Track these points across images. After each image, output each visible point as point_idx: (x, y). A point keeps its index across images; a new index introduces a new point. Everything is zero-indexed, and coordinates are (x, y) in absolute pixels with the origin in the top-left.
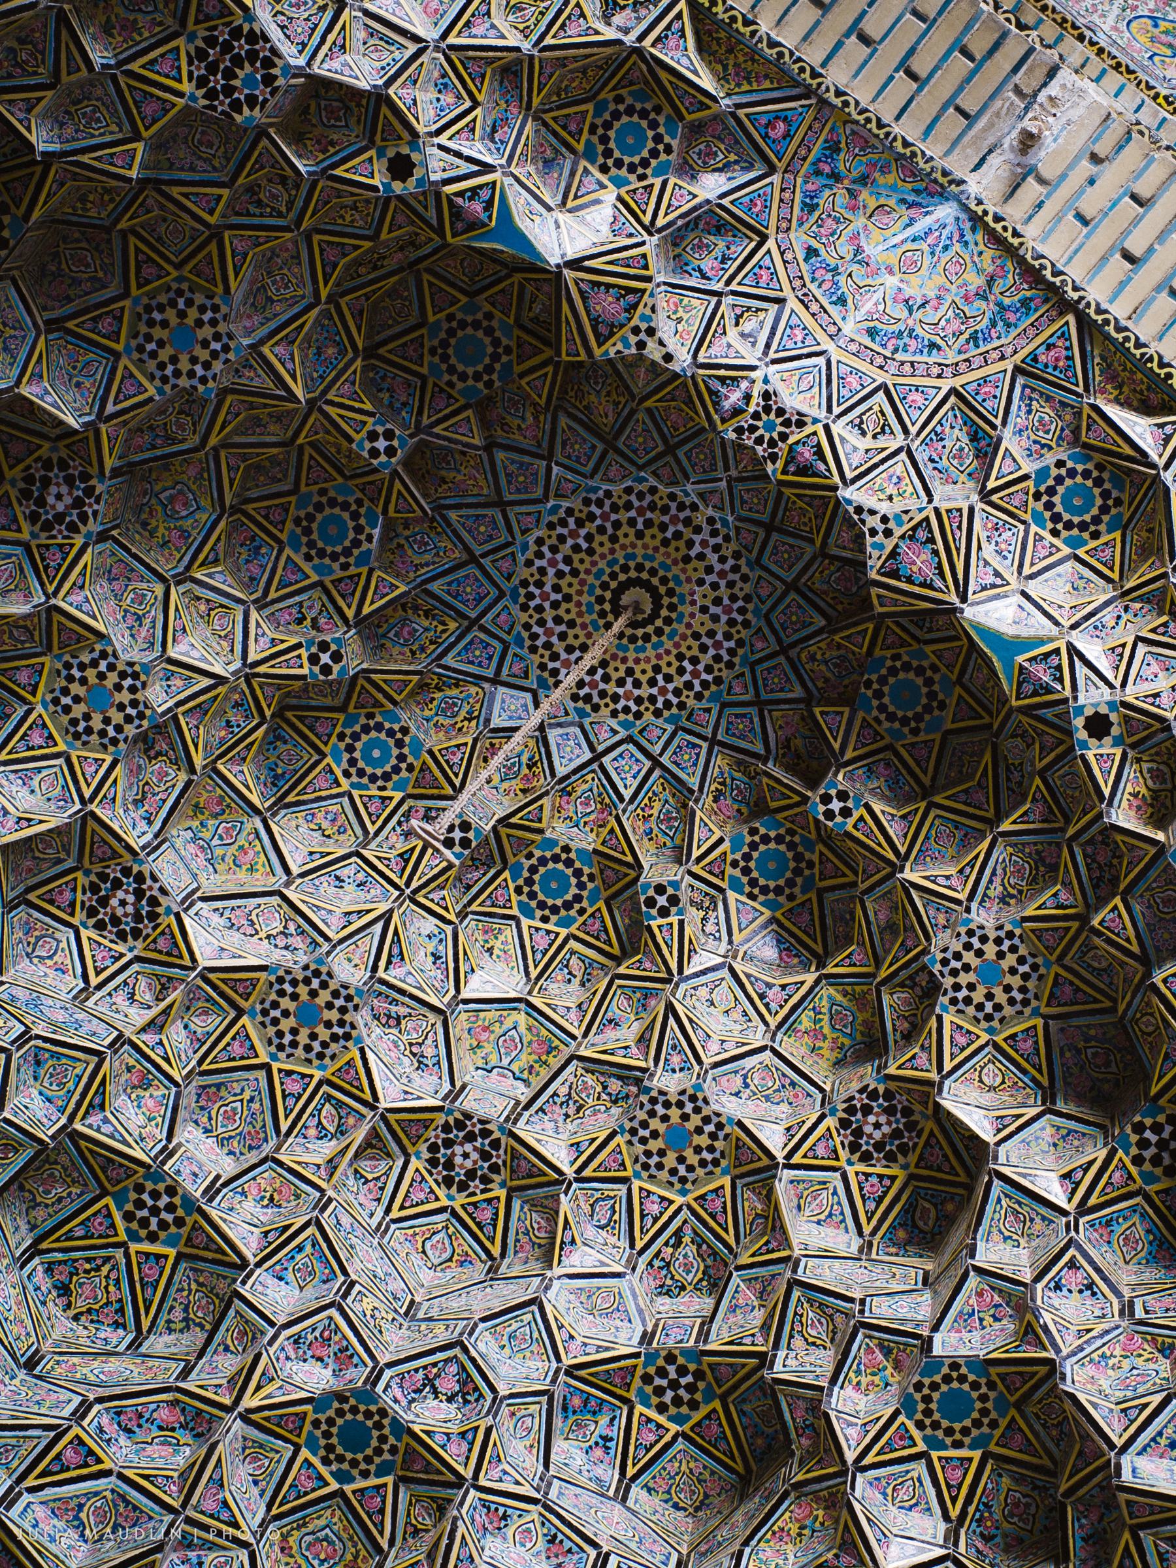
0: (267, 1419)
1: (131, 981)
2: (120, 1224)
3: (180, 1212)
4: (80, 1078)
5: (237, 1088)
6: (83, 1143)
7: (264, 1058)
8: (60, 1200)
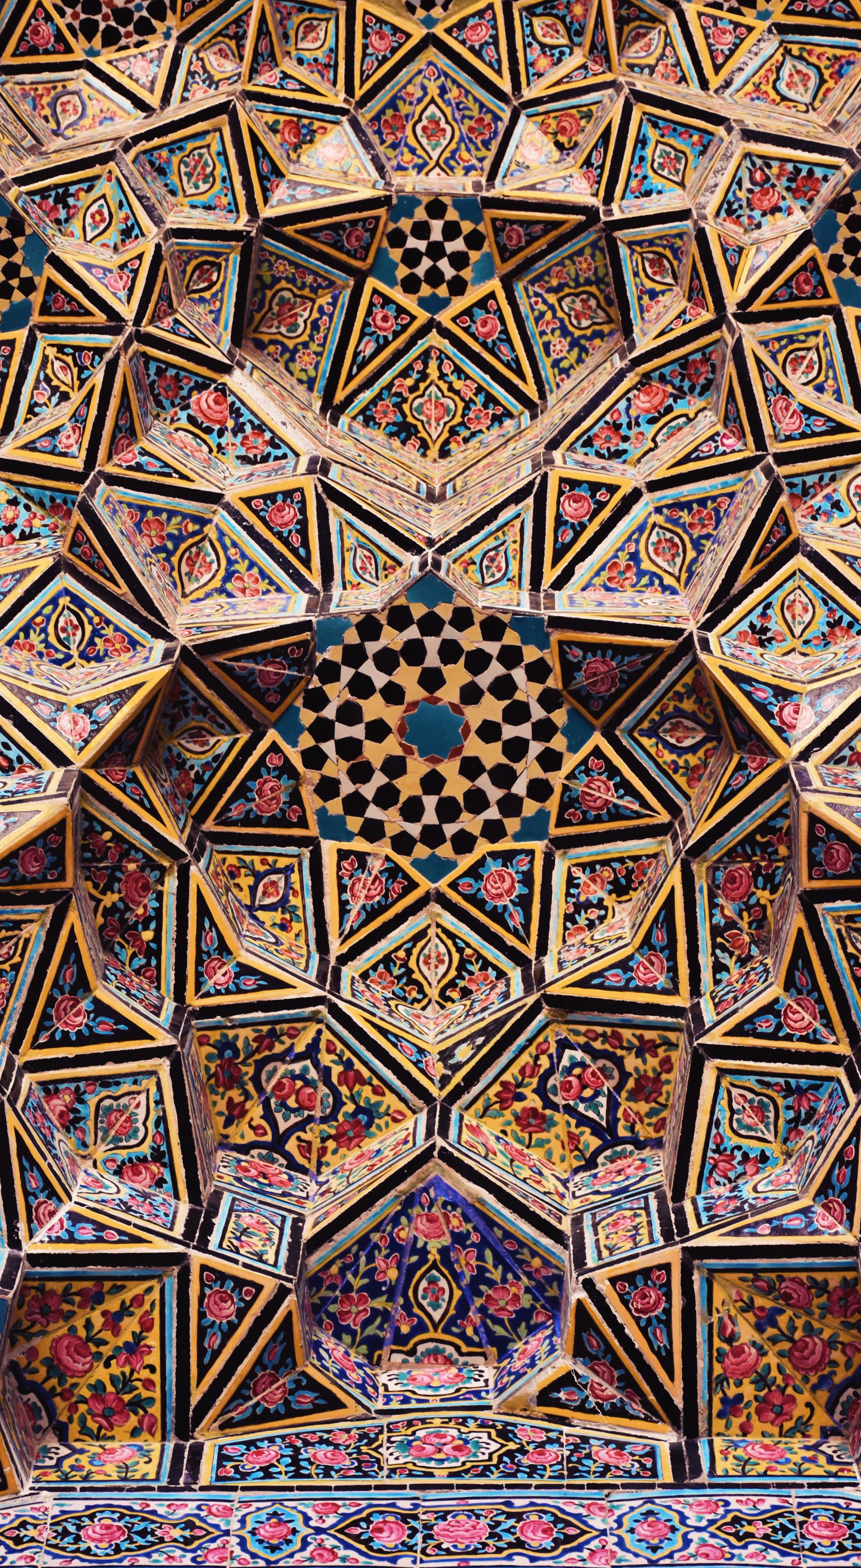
0: (772, 299)
1: (196, 67)
2: (408, 302)
3: (467, 227)
4: (223, 153)
5: (415, 90)
6: (289, 230)
7: (418, 33)
8: (315, 326)
